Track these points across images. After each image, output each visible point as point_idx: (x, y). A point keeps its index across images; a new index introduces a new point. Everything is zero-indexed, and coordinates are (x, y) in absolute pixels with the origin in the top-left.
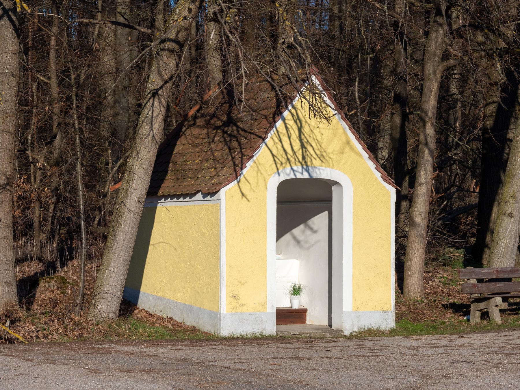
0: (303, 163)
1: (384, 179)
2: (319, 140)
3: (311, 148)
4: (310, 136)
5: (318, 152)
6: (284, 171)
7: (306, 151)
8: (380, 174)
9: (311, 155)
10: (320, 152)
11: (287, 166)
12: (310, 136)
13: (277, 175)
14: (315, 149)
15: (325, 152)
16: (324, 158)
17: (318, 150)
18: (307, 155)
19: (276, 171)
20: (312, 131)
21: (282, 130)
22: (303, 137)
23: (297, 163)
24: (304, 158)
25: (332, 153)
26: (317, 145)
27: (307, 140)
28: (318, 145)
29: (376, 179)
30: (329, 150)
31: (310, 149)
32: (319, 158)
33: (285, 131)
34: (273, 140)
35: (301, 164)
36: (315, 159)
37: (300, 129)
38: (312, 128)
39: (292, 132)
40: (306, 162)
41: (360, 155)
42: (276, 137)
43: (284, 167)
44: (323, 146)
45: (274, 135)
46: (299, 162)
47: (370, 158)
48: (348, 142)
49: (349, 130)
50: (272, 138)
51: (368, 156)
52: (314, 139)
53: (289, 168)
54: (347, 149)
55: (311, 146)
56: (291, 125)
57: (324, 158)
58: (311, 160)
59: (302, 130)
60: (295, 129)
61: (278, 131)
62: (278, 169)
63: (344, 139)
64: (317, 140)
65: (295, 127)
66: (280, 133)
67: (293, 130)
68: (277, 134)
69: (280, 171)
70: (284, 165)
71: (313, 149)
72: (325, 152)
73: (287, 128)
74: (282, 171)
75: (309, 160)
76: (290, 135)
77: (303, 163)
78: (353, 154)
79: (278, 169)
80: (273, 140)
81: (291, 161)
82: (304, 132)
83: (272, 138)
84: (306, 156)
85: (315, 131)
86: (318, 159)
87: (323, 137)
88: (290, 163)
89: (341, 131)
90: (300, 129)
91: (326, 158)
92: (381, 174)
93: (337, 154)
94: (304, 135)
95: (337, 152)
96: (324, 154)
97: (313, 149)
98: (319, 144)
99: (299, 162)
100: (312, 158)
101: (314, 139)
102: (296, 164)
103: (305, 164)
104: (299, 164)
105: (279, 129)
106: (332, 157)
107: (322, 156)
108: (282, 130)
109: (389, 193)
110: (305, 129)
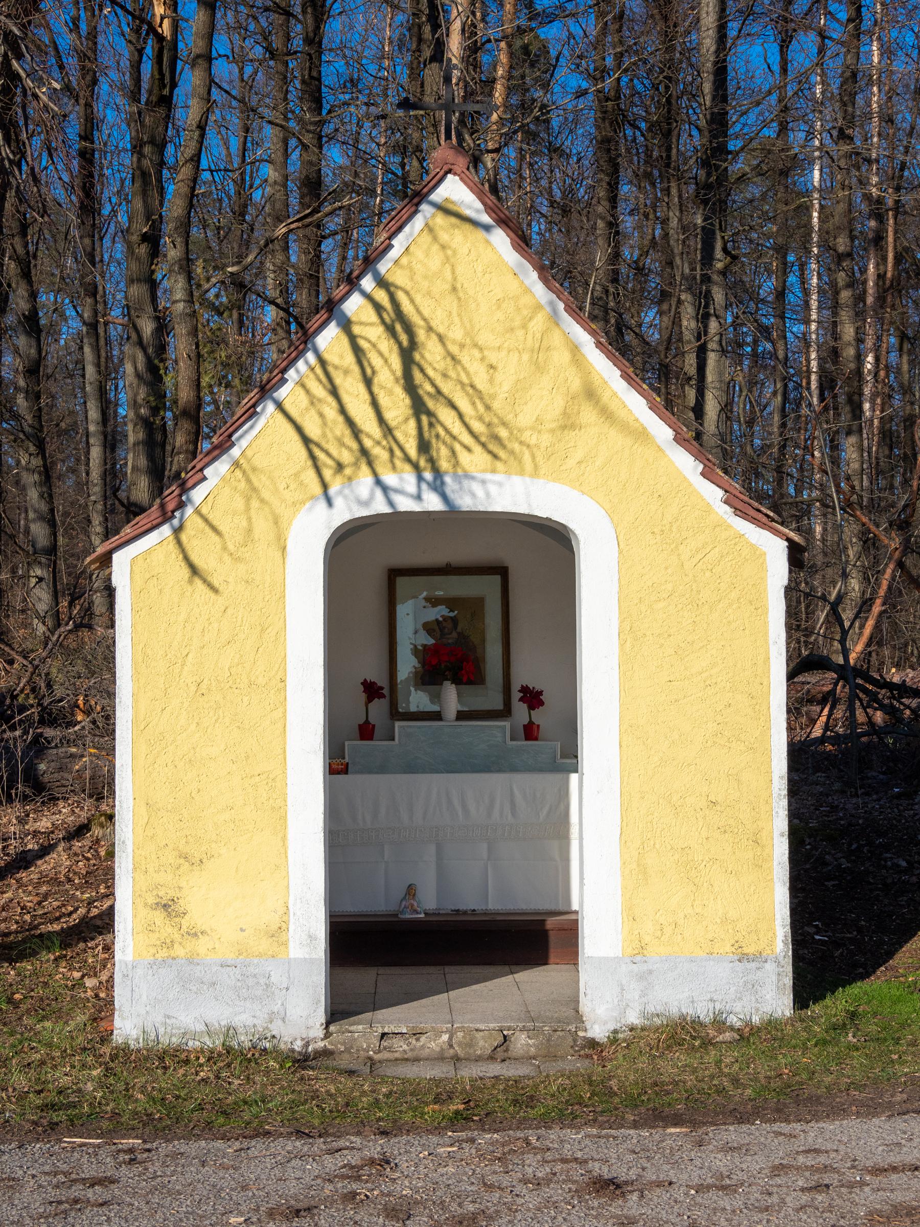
0: (422, 463)
1: (739, 512)
2: (480, 386)
3: (453, 413)
4: (445, 375)
5: (477, 427)
6: (347, 491)
7: (431, 425)
8: (720, 493)
9: (454, 438)
10: (489, 425)
11: (361, 474)
12: (445, 375)
13: (322, 504)
14: (467, 419)
15: (504, 424)
16: (504, 447)
17: (480, 419)
18: (438, 436)
19: (317, 489)
20: (453, 358)
21: (341, 357)
22: (418, 376)
23: (398, 463)
24: (424, 446)
25: (532, 428)
26: (474, 404)
27: (434, 385)
28: (478, 402)
29: (708, 509)
30: (524, 419)
31: (446, 415)
32: (484, 445)
33: (349, 359)
34: (308, 392)
35: (416, 467)
36: (468, 449)
37: (408, 354)
38: (454, 349)
39: (376, 361)
40: (432, 461)
41: (642, 435)
42: (320, 381)
43: (350, 479)
44: (496, 405)
45: (311, 376)
46: (408, 459)
47: (679, 439)
48: (590, 394)
49: (598, 351)
50: (303, 386)
51: (669, 433)
52: (462, 384)
53: (369, 480)
54: (588, 415)
55: (453, 406)
56: (373, 340)
57: (504, 447)
58: (453, 452)
59: (417, 357)
60: (386, 354)
61: (322, 362)
62: (325, 486)
63: (576, 384)
64: (472, 386)
65: (386, 345)
66: (330, 369)
67: (381, 354)
68: (319, 370)
69: (332, 491)
70: (348, 471)
71: (461, 416)
72: (504, 424)
73: (358, 351)
74: (340, 492)
75: (444, 452)
76: (369, 371)
77: (422, 463)
78: (613, 433)
79: (325, 486)
80: (308, 392)
81: (377, 457)
82: (422, 363)
83: (303, 386)
84: (434, 441)
85: (464, 358)
86: (477, 449)
87: (499, 377)
88: (370, 464)
89: (561, 356)
90: (408, 354)
91: (509, 445)
92: (726, 491)
93: (552, 431)
94: (422, 370)
95: (554, 425)
96: (503, 433)
97: (461, 416)
98: (481, 399)
99: (408, 459)
100: (458, 447)
101: (462, 384)
102: (394, 468)
103: (429, 466)
104: (408, 467)
105: (327, 356)
106: (533, 441)
107: (496, 438)
108: (341, 357)
109: (758, 556)
110: (427, 355)
